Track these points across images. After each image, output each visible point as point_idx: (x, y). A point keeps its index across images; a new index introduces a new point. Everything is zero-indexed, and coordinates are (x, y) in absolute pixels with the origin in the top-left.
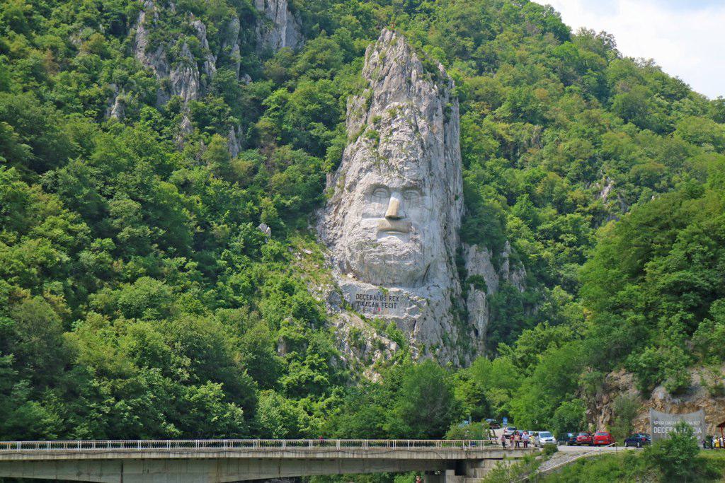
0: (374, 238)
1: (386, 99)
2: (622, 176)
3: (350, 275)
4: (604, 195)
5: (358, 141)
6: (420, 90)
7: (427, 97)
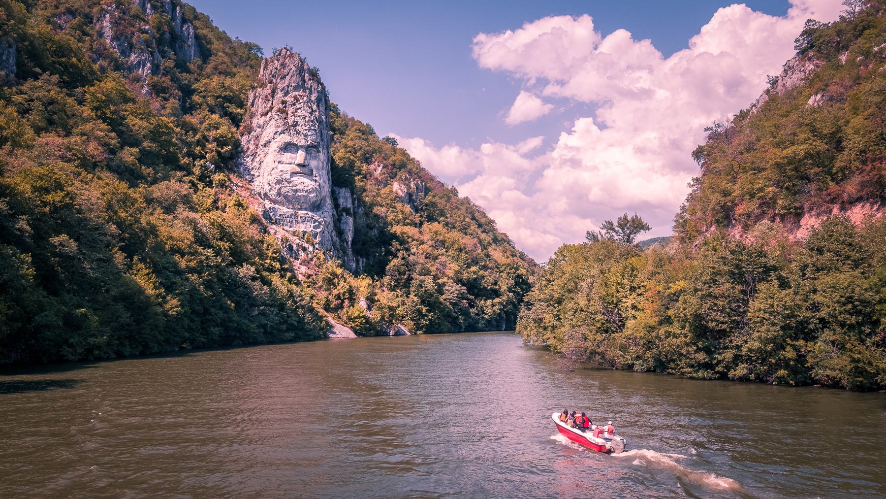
0: (289, 177)
5: (269, 114)
6: (311, 86)
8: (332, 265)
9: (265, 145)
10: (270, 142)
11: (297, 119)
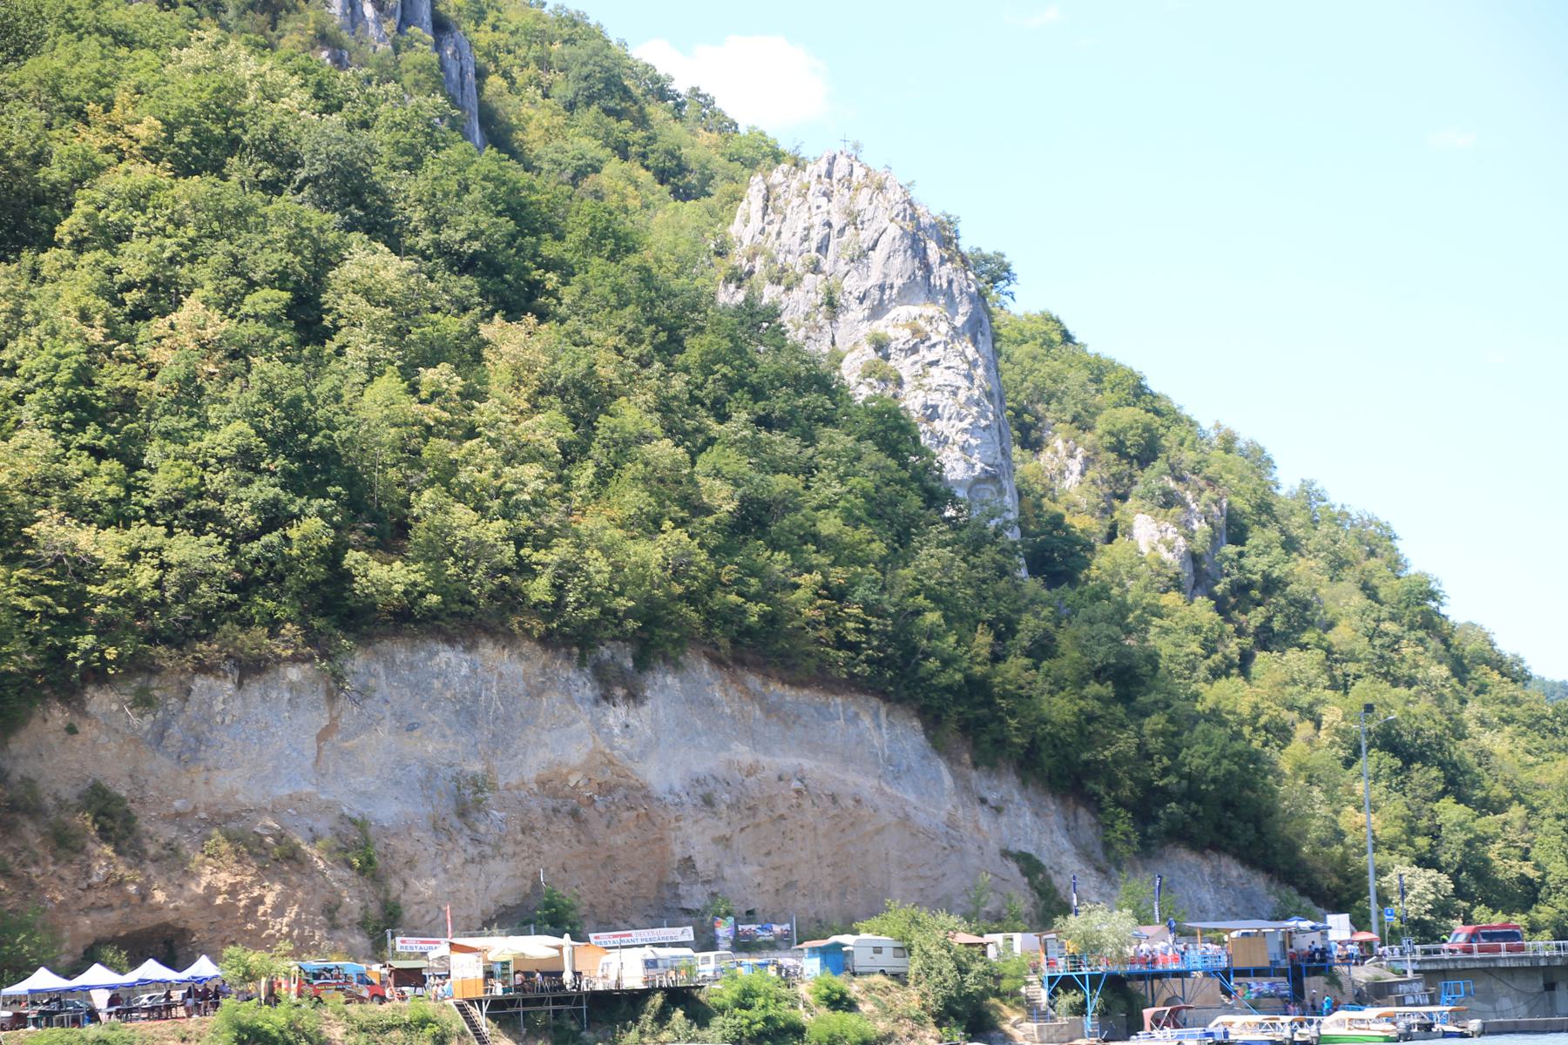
1: (881, 300)
2: (1089, 437)
4: (1072, 481)
6: (950, 282)
7: (965, 299)
11: (934, 398)
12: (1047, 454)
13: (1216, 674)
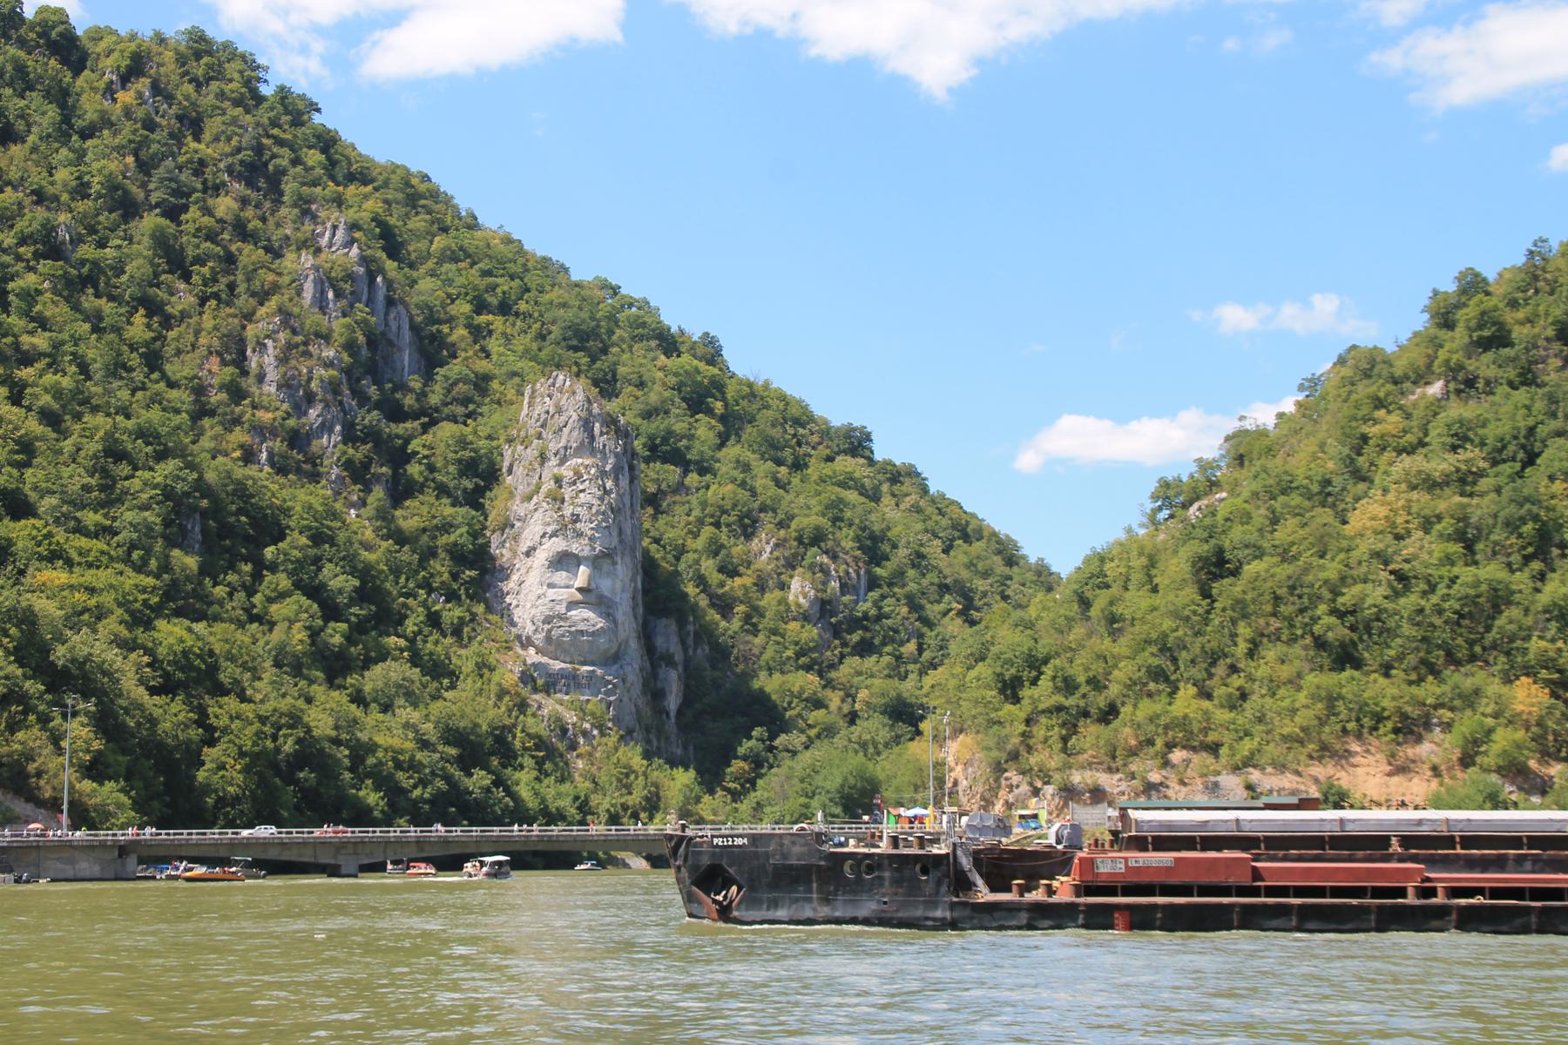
0: (563, 611)
2: (782, 532)
3: (532, 651)
4: (765, 556)
6: (604, 446)
8: (633, 756)
9: (528, 554)
10: (534, 549)
12: (756, 541)
13: (799, 668)
